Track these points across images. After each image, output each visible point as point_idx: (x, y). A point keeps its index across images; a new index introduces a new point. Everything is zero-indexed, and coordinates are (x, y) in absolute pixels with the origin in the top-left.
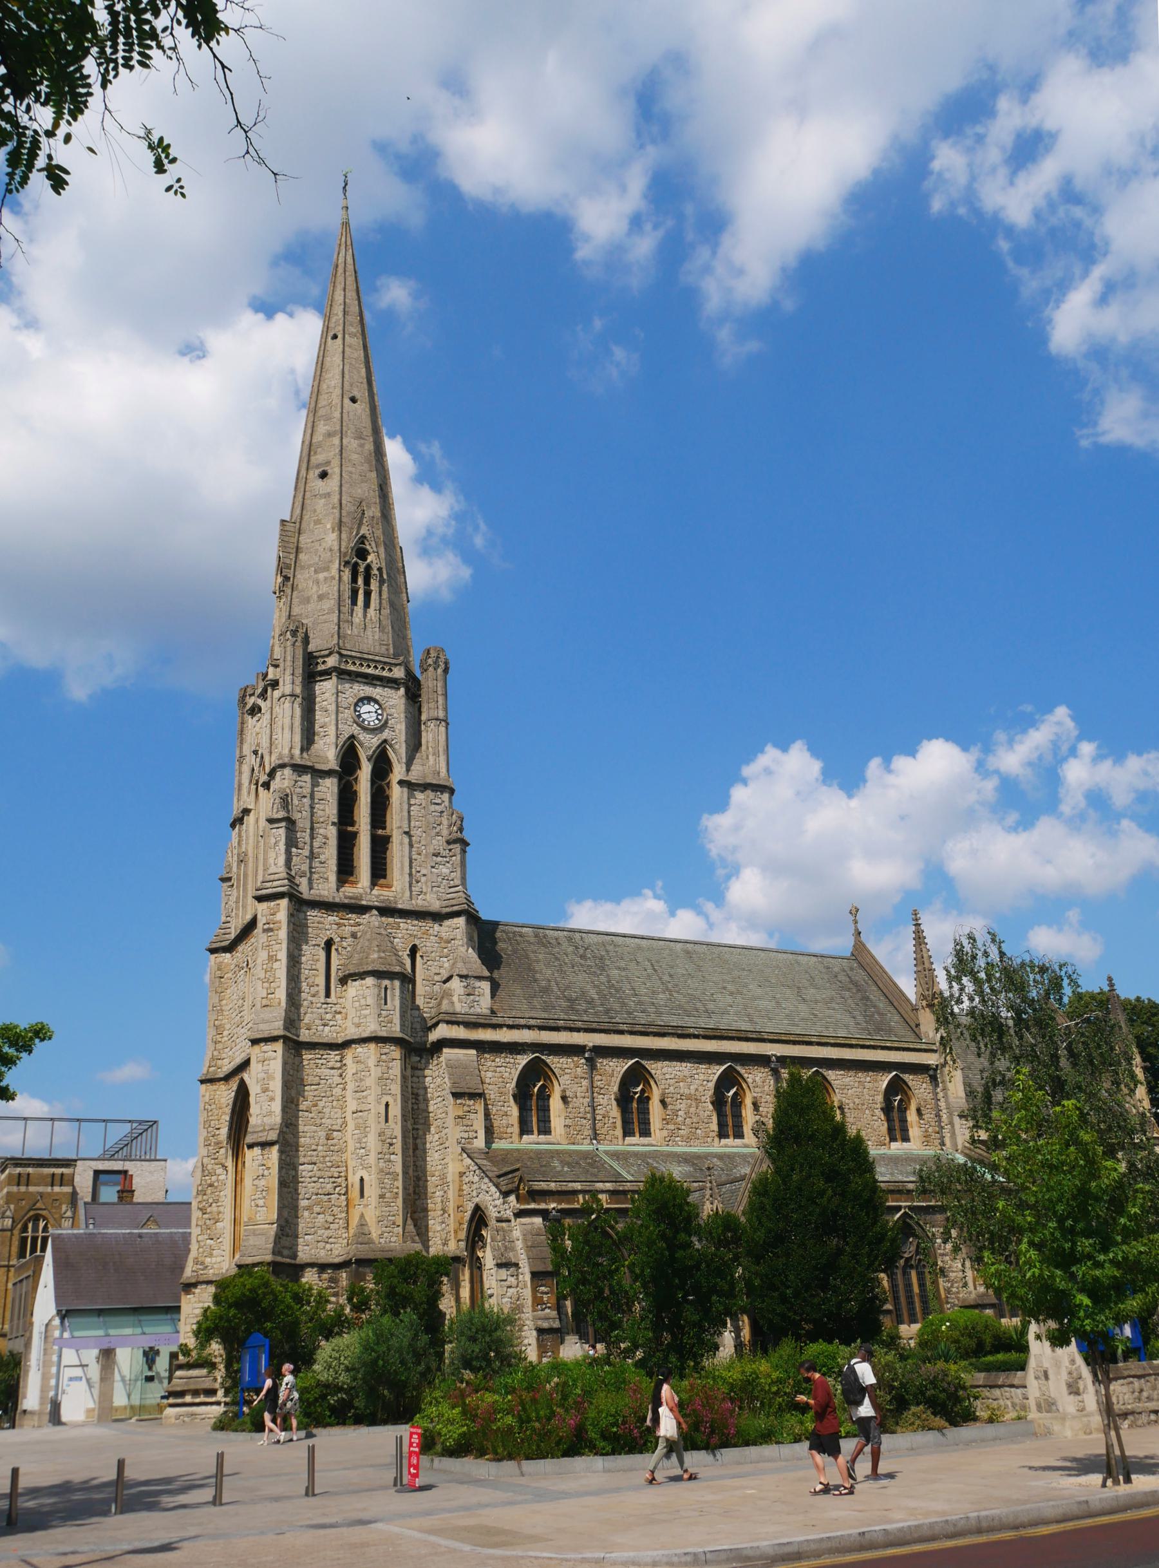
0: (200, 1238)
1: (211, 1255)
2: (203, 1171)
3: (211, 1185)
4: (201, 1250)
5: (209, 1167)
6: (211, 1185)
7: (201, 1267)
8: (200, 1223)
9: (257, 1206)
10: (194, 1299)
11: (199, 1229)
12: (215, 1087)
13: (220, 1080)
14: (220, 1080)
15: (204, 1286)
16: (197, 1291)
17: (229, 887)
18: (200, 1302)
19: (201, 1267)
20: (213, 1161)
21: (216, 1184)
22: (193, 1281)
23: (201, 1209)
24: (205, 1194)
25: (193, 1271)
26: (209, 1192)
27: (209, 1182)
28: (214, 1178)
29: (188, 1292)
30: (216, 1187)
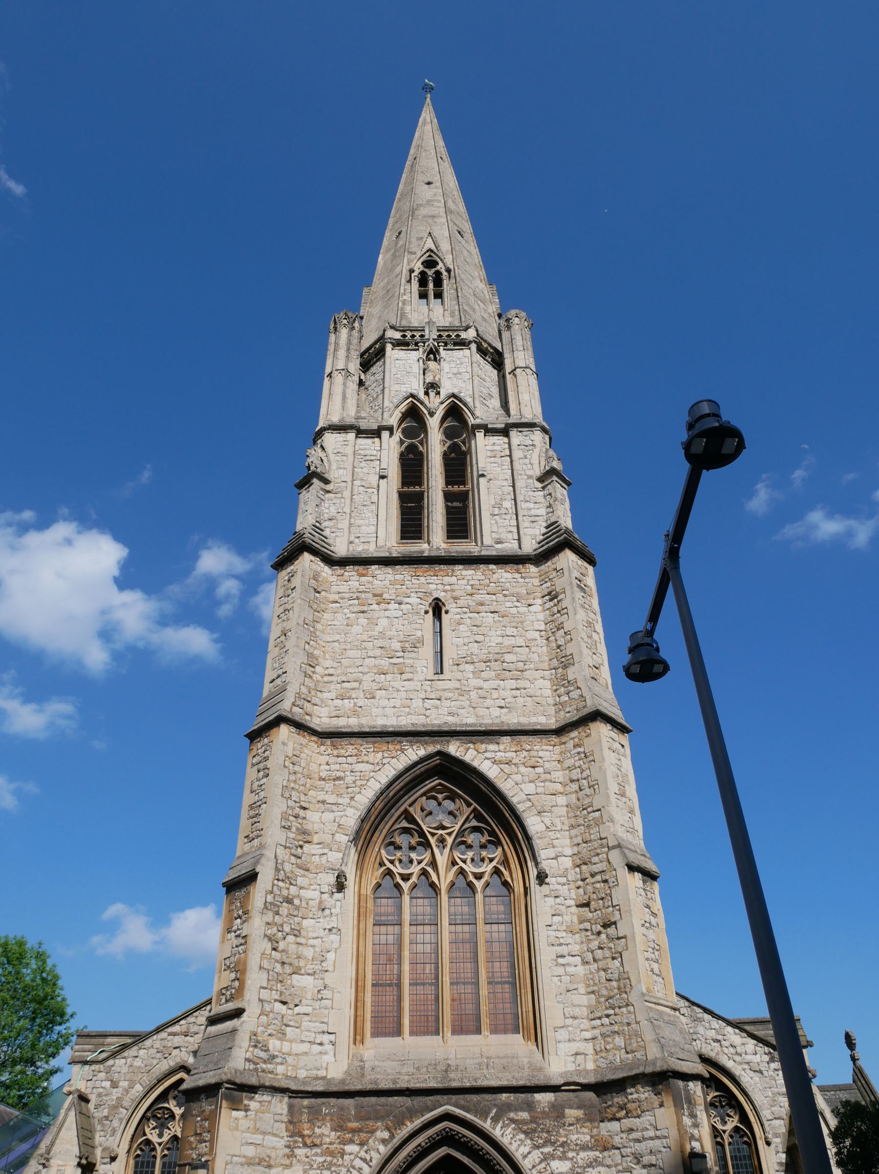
0: (264, 994)
1: (282, 1035)
2: (277, 870)
3: (289, 901)
4: (264, 1018)
5: (288, 867)
6: (289, 901)
7: (263, 1055)
8: (266, 964)
9: (652, 970)
10: (244, 1124)
11: (265, 975)
12: (304, 741)
13: (313, 732)
14: (313, 732)
15: (267, 1098)
16: (253, 1105)
17: (322, 489)
18: (257, 1131)
19: (263, 1055)
20: (293, 860)
21: (296, 902)
22: (253, 1081)
23: (270, 939)
24: (277, 913)
25: (248, 1060)
26: (285, 909)
27: (285, 893)
28: (293, 890)
29: (236, 1105)
30: (297, 908)
